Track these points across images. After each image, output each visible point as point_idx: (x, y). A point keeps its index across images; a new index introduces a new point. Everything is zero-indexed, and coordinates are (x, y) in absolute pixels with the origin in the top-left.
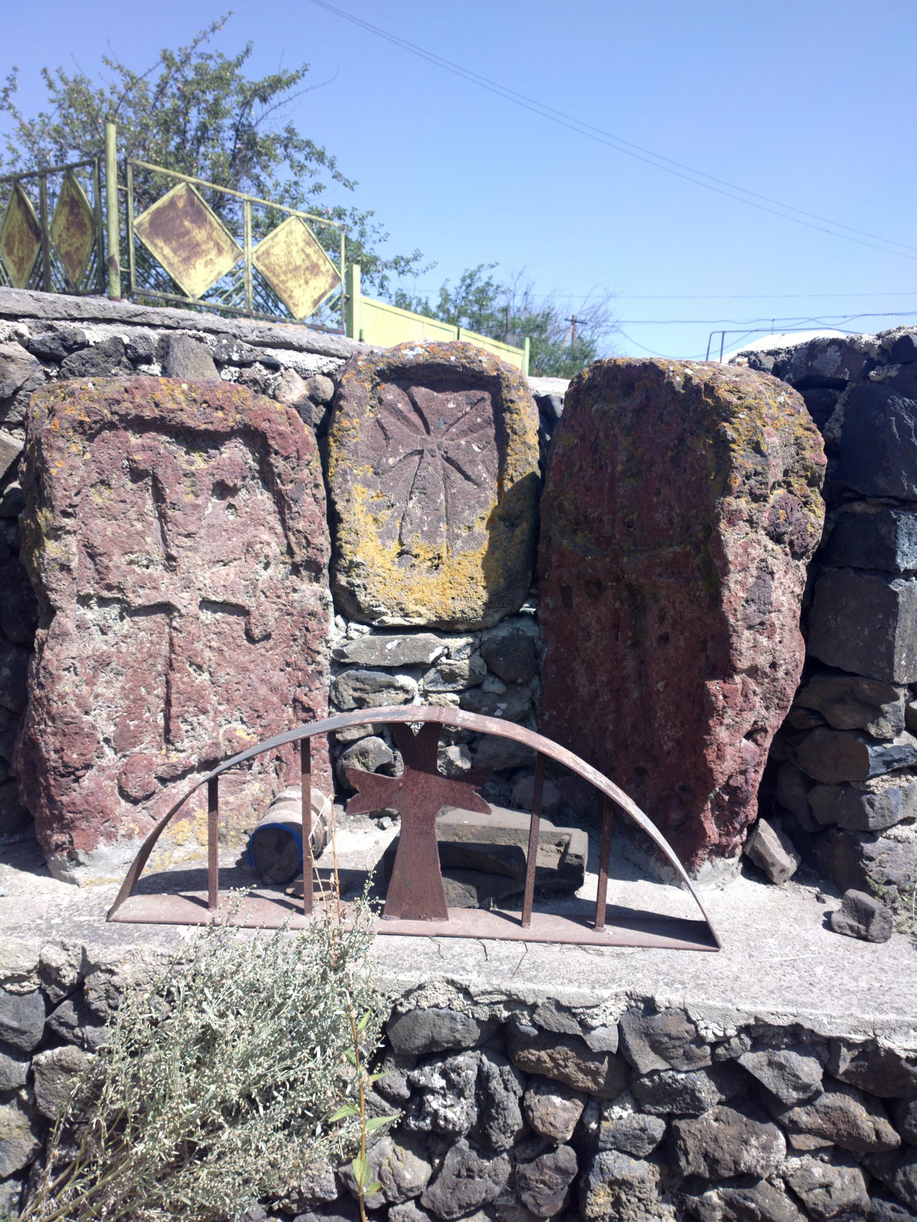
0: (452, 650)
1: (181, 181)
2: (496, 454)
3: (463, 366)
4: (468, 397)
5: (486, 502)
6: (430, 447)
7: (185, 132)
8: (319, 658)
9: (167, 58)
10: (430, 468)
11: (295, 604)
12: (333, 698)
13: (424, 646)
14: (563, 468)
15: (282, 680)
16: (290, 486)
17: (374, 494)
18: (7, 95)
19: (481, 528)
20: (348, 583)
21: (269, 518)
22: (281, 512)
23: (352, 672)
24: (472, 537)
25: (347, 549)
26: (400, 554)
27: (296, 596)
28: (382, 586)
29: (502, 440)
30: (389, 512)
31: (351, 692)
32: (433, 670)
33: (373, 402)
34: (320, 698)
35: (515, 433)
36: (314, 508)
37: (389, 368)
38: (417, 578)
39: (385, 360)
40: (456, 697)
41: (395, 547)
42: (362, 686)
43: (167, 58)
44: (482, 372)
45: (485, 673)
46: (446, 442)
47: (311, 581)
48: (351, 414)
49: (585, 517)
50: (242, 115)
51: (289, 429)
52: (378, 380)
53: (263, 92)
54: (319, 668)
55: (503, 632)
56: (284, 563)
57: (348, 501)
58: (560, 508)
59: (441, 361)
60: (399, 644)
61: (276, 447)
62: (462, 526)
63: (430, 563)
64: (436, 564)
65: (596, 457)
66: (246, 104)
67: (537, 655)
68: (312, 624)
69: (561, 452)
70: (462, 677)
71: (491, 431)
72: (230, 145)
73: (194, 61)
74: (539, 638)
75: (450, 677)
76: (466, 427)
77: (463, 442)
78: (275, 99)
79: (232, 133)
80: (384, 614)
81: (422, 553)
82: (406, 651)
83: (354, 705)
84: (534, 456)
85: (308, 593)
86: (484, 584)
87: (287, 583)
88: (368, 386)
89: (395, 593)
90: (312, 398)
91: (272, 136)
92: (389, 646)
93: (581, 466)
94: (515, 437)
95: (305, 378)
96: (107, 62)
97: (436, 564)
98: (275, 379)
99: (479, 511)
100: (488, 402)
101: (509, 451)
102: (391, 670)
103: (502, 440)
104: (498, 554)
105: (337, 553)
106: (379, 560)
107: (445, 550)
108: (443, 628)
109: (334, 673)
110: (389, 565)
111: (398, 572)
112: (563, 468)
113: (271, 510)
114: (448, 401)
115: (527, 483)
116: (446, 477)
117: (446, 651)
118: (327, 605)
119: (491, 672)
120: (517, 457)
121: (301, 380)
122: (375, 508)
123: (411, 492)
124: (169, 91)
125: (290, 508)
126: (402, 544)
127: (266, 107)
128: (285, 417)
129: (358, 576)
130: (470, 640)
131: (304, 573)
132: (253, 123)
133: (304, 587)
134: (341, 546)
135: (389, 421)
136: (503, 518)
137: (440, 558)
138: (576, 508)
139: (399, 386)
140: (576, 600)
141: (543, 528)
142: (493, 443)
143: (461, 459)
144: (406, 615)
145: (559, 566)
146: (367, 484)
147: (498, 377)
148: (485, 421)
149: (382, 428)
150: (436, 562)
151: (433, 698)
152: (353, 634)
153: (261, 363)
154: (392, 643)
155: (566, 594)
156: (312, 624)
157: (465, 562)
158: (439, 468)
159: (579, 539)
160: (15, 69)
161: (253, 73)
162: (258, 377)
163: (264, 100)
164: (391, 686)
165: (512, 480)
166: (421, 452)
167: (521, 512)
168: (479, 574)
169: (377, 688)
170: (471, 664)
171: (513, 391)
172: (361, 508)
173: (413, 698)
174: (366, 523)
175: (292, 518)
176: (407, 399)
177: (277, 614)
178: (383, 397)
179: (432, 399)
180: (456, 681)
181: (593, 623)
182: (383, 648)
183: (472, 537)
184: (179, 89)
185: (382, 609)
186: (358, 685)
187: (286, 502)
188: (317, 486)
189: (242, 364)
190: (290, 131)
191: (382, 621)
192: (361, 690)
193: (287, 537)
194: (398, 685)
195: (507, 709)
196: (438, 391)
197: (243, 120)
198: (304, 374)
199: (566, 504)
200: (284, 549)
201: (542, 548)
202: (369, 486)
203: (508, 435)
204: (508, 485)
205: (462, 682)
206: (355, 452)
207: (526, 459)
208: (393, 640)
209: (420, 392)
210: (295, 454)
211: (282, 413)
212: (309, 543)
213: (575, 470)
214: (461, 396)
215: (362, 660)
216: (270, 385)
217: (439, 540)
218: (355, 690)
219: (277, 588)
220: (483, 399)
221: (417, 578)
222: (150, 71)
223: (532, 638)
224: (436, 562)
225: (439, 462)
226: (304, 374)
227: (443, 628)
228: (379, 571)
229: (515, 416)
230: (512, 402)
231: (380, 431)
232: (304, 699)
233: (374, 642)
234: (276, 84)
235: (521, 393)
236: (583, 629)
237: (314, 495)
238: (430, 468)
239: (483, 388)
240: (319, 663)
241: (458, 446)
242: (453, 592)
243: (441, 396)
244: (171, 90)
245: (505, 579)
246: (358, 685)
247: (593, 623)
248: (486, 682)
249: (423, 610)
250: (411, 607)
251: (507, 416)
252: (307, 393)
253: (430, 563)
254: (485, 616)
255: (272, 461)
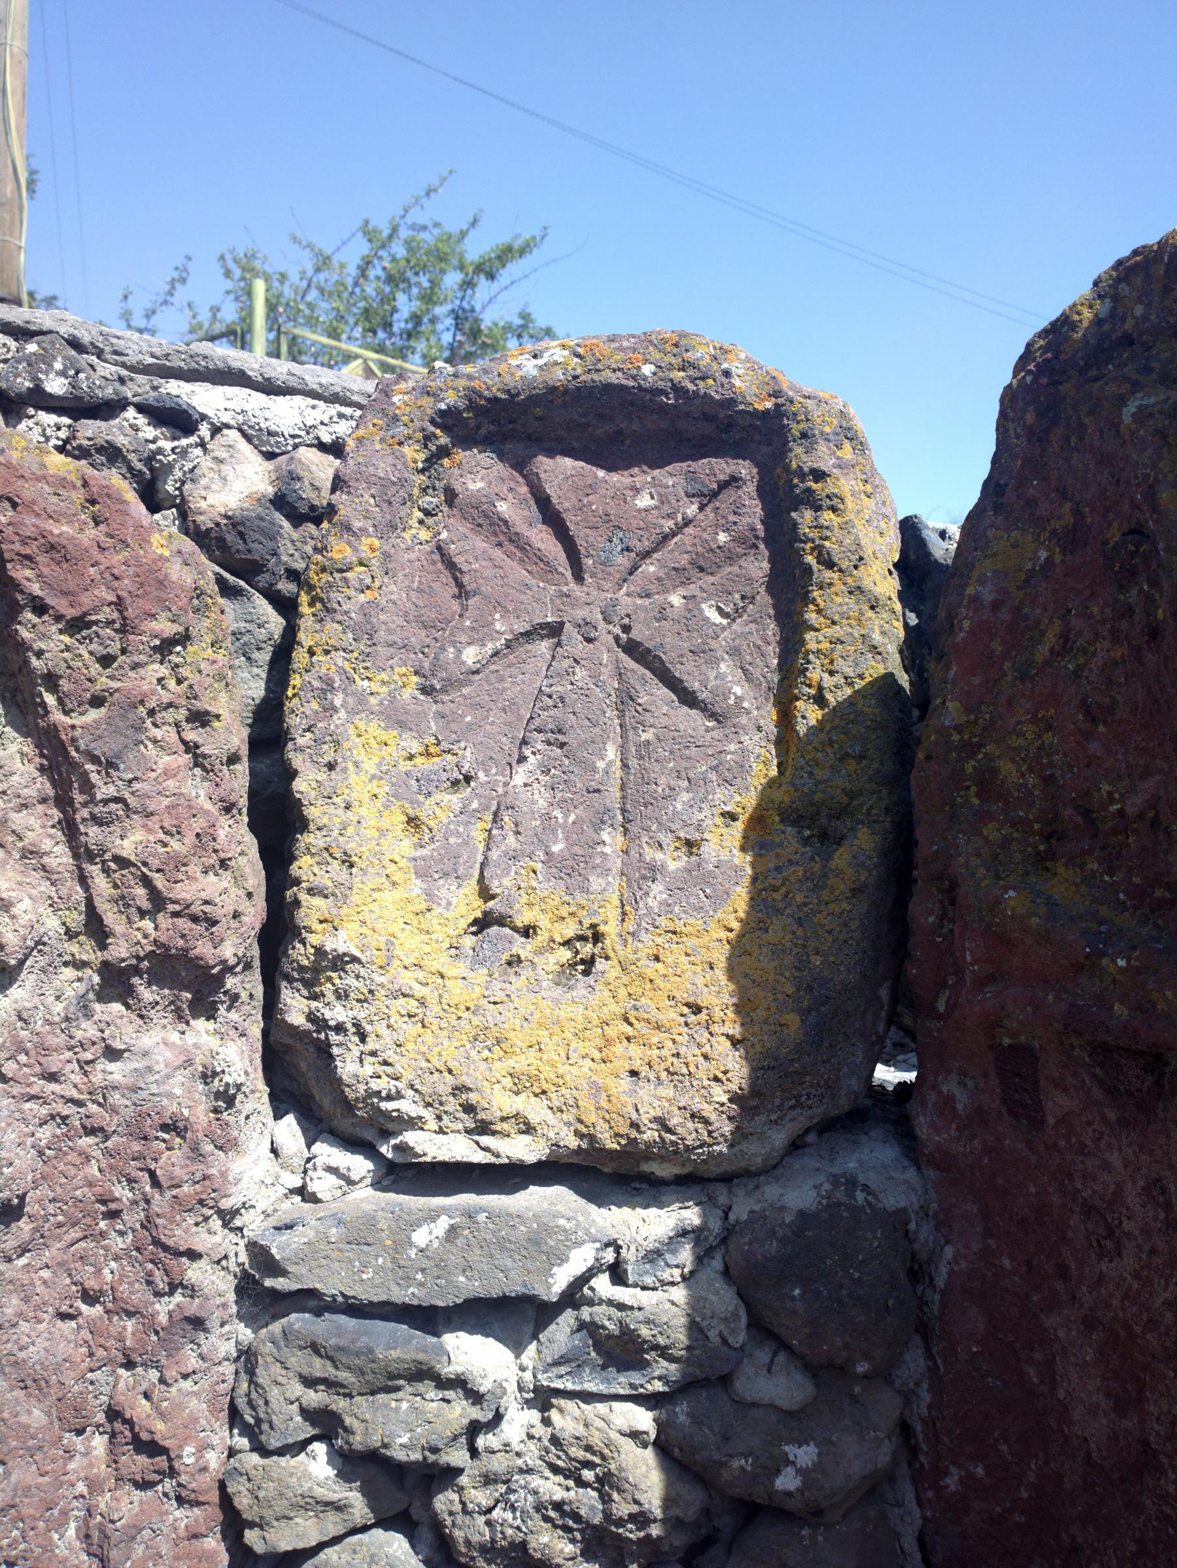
0: (630, 1255)
1: (357, 357)
2: (772, 627)
3: (677, 389)
4: (691, 476)
5: (742, 767)
6: (580, 614)
7: (391, 325)
8: (195, 1273)
9: (369, 233)
10: (580, 673)
11: (116, 1098)
12: (241, 1403)
13: (535, 1241)
14: (997, 646)
15: (63, 1349)
16: (94, 714)
17: (415, 747)
18: (173, 288)
19: (725, 847)
20: (311, 1017)
21: (19, 820)
22: (63, 801)
23: (297, 1320)
24: (697, 875)
25: (311, 910)
26: (482, 924)
27: (117, 1071)
28: (414, 1029)
29: (790, 589)
30: (454, 800)
31: (297, 1389)
32: (567, 1319)
33: (429, 501)
34: (199, 1406)
35: (830, 565)
36: (198, 790)
37: (472, 406)
38: (524, 1003)
39: (462, 383)
40: (644, 1419)
41: (464, 904)
42: (330, 1372)
43: (369, 233)
44: (731, 402)
45: (740, 1338)
46: (626, 601)
47: (180, 1017)
48: (357, 524)
49: (1087, 814)
50: (463, 298)
51: (92, 532)
52: (444, 440)
53: (488, 269)
54: (193, 1307)
55: (799, 1194)
56: (80, 965)
57: (331, 766)
58: (987, 782)
59: (614, 378)
60: (453, 1229)
61: (36, 589)
62: (666, 839)
63: (565, 955)
64: (585, 954)
65: (1132, 596)
66: (468, 284)
67: (918, 1272)
68: (172, 1160)
69: (988, 594)
70: (663, 1352)
71: (758, 567)
72: (447, 338)
73: (404, 233)
74: (924, 1210)
75: (621, 1350)
76: (684, 560)
77: (676, 600)
78: (506, 275)
79: (449, 321)
80: (413, 1123)
81: (544, 922)
82: (475, 1255)
83: (311, 1431)
84: (889, 629)
85: (162, 1058)
86: (736, 1031)
87: (87, 1030)
88: (414, 454)
89: (449, 1051)
90: (281, 502)
91: (502, 324)
92: (421, 1237)
93: (1065, 637)
94: (828, 575)
95: (270, 456)
96: (295, 239)
97: (585, 954)
98: (184, 453)
99: (720, 794)
100: (751, 488)
101: (812, 617)
102: (429, 1319)
103: (790, 589)
104: (779, 929)
105: (279, 929)
106: (410, 944)
107: (613, 914)
108: (606, 1171)
109: (251, 1319)
110: (440, 961)
111: (466, 983)
112: (997, 646)
113: (30, 792)
114: (636, 490)
115: (871, 708)
116: (626, 698)
117: (609, 1256)
118: (227, 1098)
119: (761, 1329)
120: (836, 632)
121: (259, 459)
122: (409, 790)
123: (524, 742)
124: (372, 273)
125: (87, 787)
126: (486, 894)
127: (495, 286)
128: (78, 496)
129: (342, 995)
130: (692, 1216)
131: (147, 994)
132: (478, 308)
133: (149, 1039)
134: (297, 903)
135: (473, 549)
136: (793, 816)
137: (597, 937)
138: (1047, 780)
139: (501, 457)
140: (1057, 1103)
141: (927, 846)
142: (764, 598)
143: (671, 646)
144: (484, 1128)
145: (988, 980)
146: (397, 719)
147: (778, 412)
148: (740, 540)
149: (451, 566)
150: (587, 949)
151: (568, 1419)
152: (323, 1184)
153: (141, 408)
154: (433, 1221)
155: (1016, 1069)
156: (172, 1160)
157: (674, 954)
158: (606, 674)
159: (1062, 885)
160: (189, 258)
161: (476, 249)
162: (121, 441)
163: (491, 276)
164: (422, 1373)
165: (819, 700)
166: (554, 631)
167: (852, 795)
168: (719, 994)
169: (382, 1381)
170: (696, 1305)
171: (822, 448)
172: (374, 787)
173: (498, 1417)
174: (383, 832)
175: (96, 820)
176: (524, 489)
177: (45, 1134)
178: (458, 488)
179: (591, 489)
180: (641, 1365)
181: (1132, 1197)
182: (402, 1242)
183: (697, 875)
184: (384, 269)
185: (407, 1106)
186: (319, 1367)
187: (75, 766)
188: (201, 718)
189: (79, 408)
190: (526, 317)
191: (402, 1148)
192: (330, 1384)
193: (83, 880)
194: (448, 1371)
195: (818, 1467)
196: (610, 469)
197: (465, 304)
198: (267, 445)
199: (1008, 769)
200: (76, 919)
201: (924, 911)
202: (402, 725)
203: (808, 570)
204: (809, 715)
205: (663, 1367)
206: (366, 631)
207: (865, 636)
208: (432, 1216)
209: (560, 472)
210: (108, 613)
211: (63, 483)
212: (158, 901)
213: (1042, 651)
214: (672, 477)
215: (331, 1285)
216: (170, 467)
217: (596, 883)
218: (310, 1382)
219: (46, 1050)
220: (734, 481)
221: (524, 1003)
222: (344, 243)
223: (901, 1215)
224: (587, 949)
225: (606, 654)
226: (267, 445)
227: (606, 1171)
228: (407, 979)
229: (827, 516)
230: (819, 475)
231: (446, 576)
232: (141, 1409)
233: (370, 1222)
234: (506, 254)
235: (847, 453)
236: (1089, 1210)
237: (191, 748)
238: (580, 673)
239: (738, 451)
240: (192, 1291)
241: (662, 613)
242: (635, 1050)
243: (615, 477)
244: (375, 272)
245: (804, 1013)
246: (319, 1367)
247: (1132, 1197)
248: (747, 1368)
249: (536, 1110)
250: (500, 1102)
251: (805, 518)
252: (271, 491)
253: (565, 955)
254: (739, 1135)
255: (25, 634)
